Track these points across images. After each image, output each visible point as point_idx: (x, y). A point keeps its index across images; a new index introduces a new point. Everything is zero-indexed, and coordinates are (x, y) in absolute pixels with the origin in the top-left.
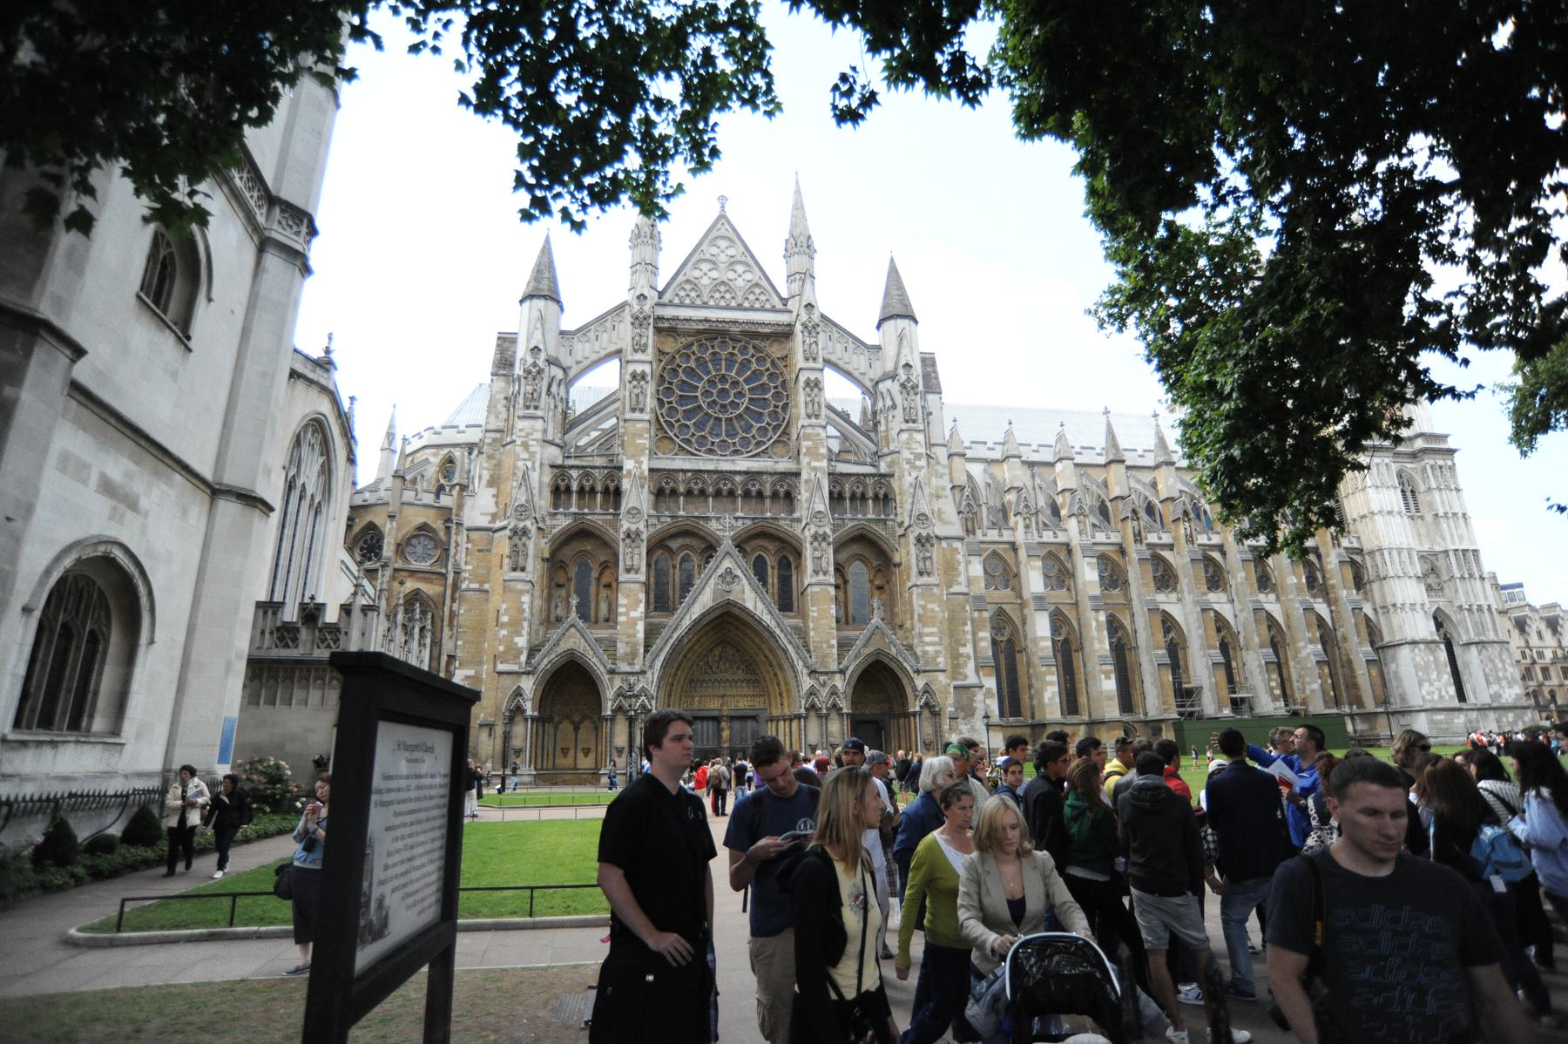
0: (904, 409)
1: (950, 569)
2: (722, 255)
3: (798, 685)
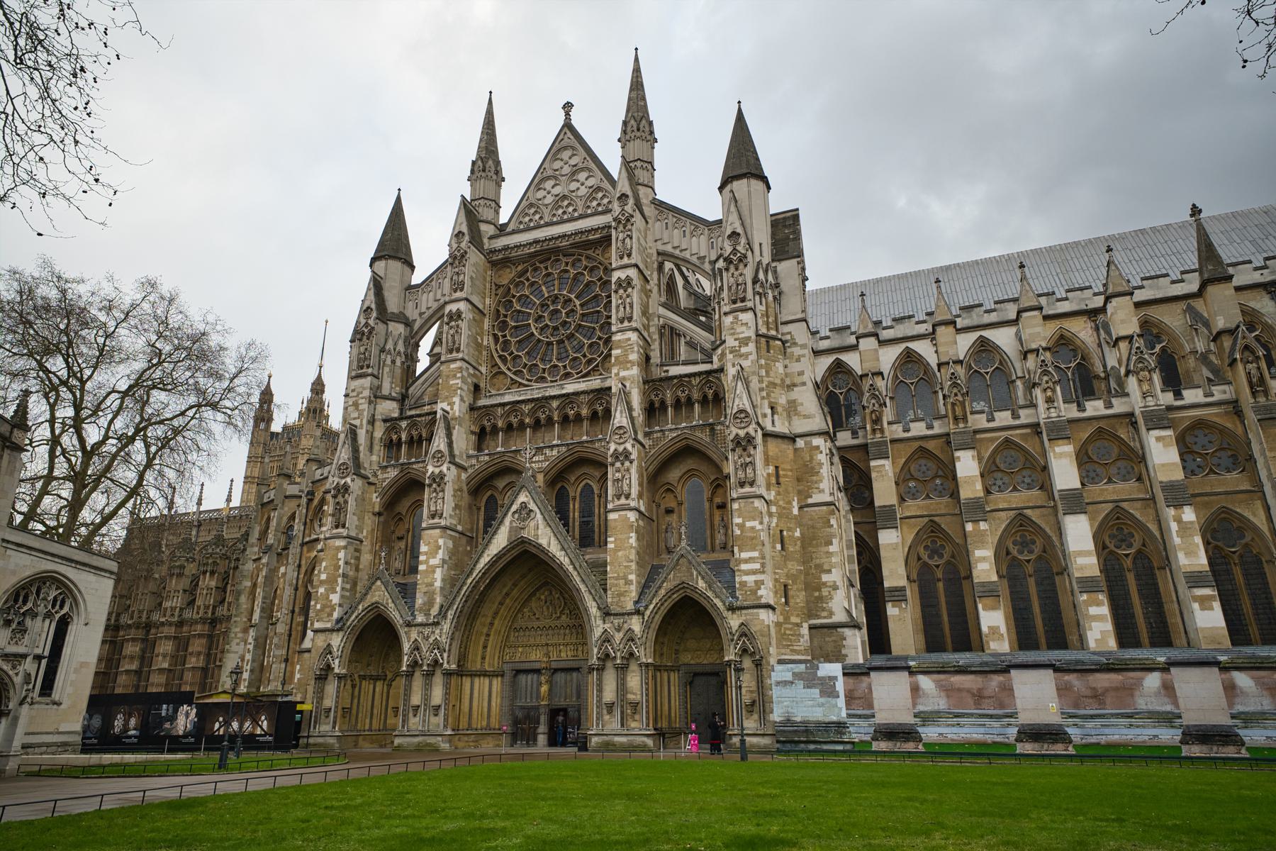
0: (730, 288)
3: (592, 630)
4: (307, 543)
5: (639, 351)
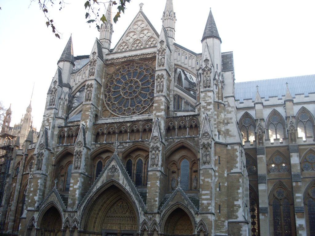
0: (204, 81)
4: (25, 174)
5: (165, 105)
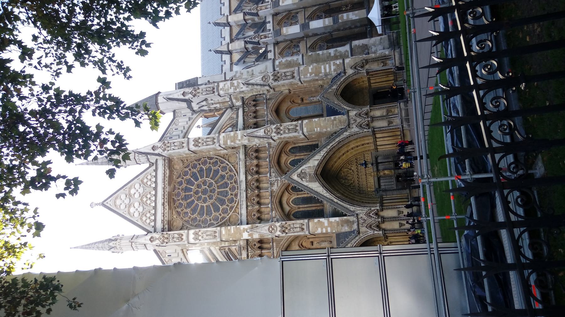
0: (207, 94)
1: (289, 65)
2: (126, 201)
